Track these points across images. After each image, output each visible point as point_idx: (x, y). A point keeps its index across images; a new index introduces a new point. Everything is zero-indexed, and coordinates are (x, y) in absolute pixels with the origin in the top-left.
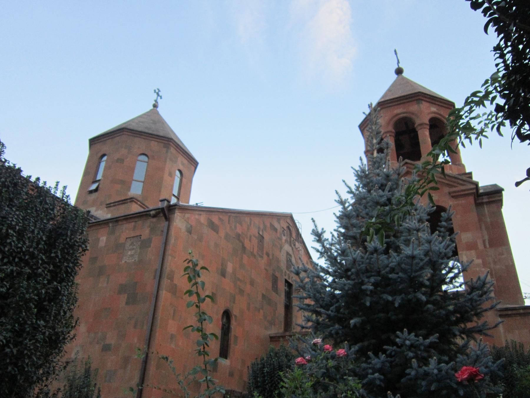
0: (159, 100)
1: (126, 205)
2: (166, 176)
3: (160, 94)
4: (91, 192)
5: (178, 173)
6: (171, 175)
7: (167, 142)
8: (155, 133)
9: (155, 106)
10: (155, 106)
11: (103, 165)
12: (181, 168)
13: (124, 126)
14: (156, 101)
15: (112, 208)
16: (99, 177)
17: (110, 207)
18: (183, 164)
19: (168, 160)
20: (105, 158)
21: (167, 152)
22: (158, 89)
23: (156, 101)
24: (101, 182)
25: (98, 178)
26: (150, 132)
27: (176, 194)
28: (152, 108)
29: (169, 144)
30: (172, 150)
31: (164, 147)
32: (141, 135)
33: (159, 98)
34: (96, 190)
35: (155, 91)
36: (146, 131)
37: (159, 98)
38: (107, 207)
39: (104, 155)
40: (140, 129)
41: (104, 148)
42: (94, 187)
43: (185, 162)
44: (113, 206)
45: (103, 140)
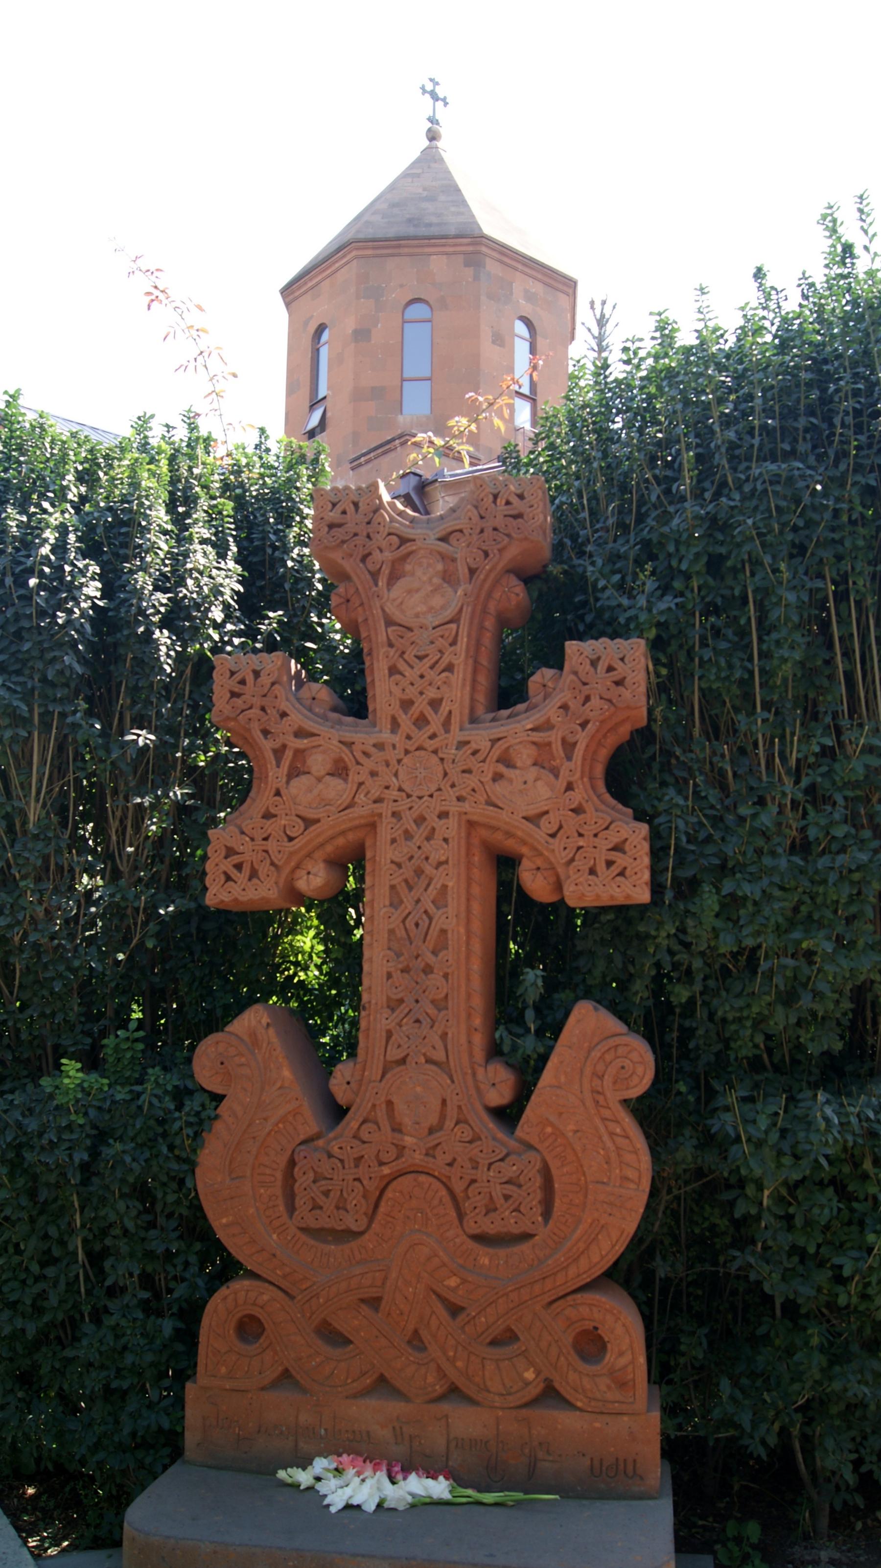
0: (442, 114)
1: (392, 455)
2: (488, 350)
3: (440, 92)
4: (311, 434)
5: (520, 328)
6: (502, 340)
7: (471, 248)
8: (434, 231)
9: (433, 136)
10: (433, 136)
11: (324, 352)
12: (527, 309)
13: (350, 236)
14: (432, 120)
15: (363, 469)
16: (322, 392)
17: (360, 465)
18: (530, 297)
19: (483, 298)
20: (325, 336)
21: (476, 278)
22: (431, 80)
23: (432, 120)
24: (328, 403)
25: (320, 396)
26: (423, 231)
27: (526, 390)
28: (426, 143)
29: (479, 253)
30: (492, 267)
31: (467, 264)
32: (399, 246)
33: (440, 104)
34: (323, 424)
35: (424, 90)
36: (411, 231)
37: (440, 104)
38: (353, 469)
39: (320, 329)
40: (391, 232)
41: (319, 308)
42: (315, 420)
43: (537, 288)
44: (368, 462)
45: (310, 284)
